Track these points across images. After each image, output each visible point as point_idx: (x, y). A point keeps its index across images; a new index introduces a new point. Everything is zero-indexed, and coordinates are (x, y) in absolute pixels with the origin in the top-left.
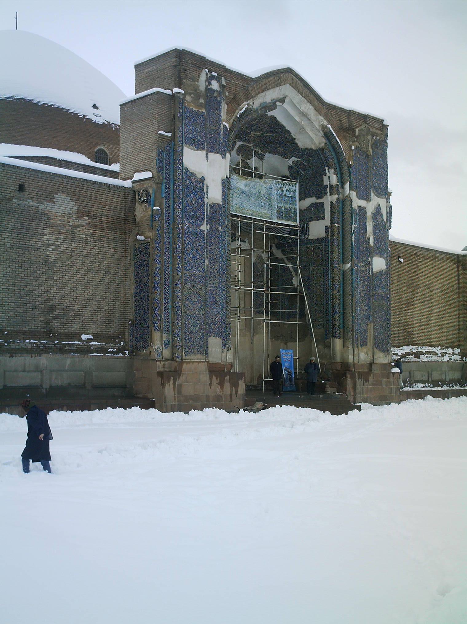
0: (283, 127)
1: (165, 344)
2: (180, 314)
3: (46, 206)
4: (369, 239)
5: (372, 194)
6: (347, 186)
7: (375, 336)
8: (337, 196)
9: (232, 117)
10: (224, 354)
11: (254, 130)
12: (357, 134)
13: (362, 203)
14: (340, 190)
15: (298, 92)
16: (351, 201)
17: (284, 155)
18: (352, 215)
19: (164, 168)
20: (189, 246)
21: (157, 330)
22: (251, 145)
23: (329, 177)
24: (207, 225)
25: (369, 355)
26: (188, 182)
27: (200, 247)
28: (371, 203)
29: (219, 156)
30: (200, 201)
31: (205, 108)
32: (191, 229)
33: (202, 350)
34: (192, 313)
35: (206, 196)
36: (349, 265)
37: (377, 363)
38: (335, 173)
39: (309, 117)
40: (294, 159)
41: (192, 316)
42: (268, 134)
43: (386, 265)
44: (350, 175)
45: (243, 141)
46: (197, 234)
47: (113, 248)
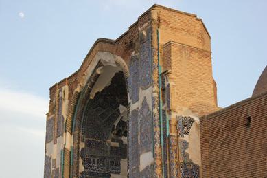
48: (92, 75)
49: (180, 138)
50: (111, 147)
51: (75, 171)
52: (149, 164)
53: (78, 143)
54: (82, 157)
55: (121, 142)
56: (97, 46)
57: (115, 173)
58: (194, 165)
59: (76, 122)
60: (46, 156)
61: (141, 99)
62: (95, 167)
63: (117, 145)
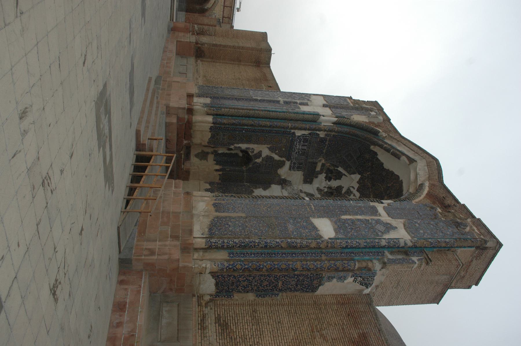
48: (398, 150)
49: (351, 274)
50: (316, 163)
51: (297, 125)
52: (321, 233)
53: (325, 131)
54: (310, 134)
55: (321, 172)
56: (432, 160)
57: (290, 166)
58: (317, 288)
59: (346, 129)
60: (310, 94)
61: (394, 222)
62: (298, 146)
63: (318, 169)
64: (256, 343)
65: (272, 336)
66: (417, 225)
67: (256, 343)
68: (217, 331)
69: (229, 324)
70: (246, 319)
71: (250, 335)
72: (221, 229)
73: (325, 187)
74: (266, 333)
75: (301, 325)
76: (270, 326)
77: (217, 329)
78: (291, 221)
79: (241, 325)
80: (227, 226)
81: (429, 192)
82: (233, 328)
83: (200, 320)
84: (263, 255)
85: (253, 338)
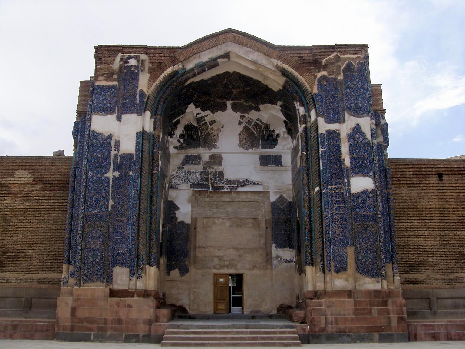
0: (251, 79)
1: (71, 274)
2: (80, 248)
3: (8, 180)
4: (344, 160)
5: (347, 115)
6: (313, 113)
7: (357, 261)
8: (304, 125)
9: (154, 82)
10: (132, 282)
11: (233, 88)
12: (323, 64)
13: (333, 127)
14: (308, 120)
15: (242, 45)
16: (317, 127)
17: (273, 102)
18: (318, 140)
19: (79, 134)
20: (92, 192)
21: (65, 263)
22: (242, 101)
23: (298, 110)
24: (114, 171)
25: (350, 282)
26: (94, 141)
27: (104, 191)
28: (345, 124)
29: (134, 116)
30: (106, 154)
31: (118, 82)
32: (95, 178)
33: (101, 278)
34: (93, 247)
35: (113, 149)
36: (317, 189)
37: (362, 291)
38: (302, 104)
39: (260, 63)
40: (279, 103)
41: (92, 249)
42: (248, 88)
43: (375, 183)
44: (314, 102)
45: (231, 100)
46: (100, 181)
47: (62, 203)
64: (423, 248)
65: (418, 236)
66: (352, 105)
67: (423, 248)
68: (415, 272)
69: (410, 264)
70: (406, 253)
71: (418, 251)
72: (371, 268)
73: (178, 141)
74: (416, 240)
75: (409, 215)
76: (410, 236)
77: (414, 272)
78: (357, 210)
79: (410, 256)
80: (367, 263)
81: (293, 68)
82: (412, 262)
83: (411, 284)
84: (387, 237)
85: (420, 249)
